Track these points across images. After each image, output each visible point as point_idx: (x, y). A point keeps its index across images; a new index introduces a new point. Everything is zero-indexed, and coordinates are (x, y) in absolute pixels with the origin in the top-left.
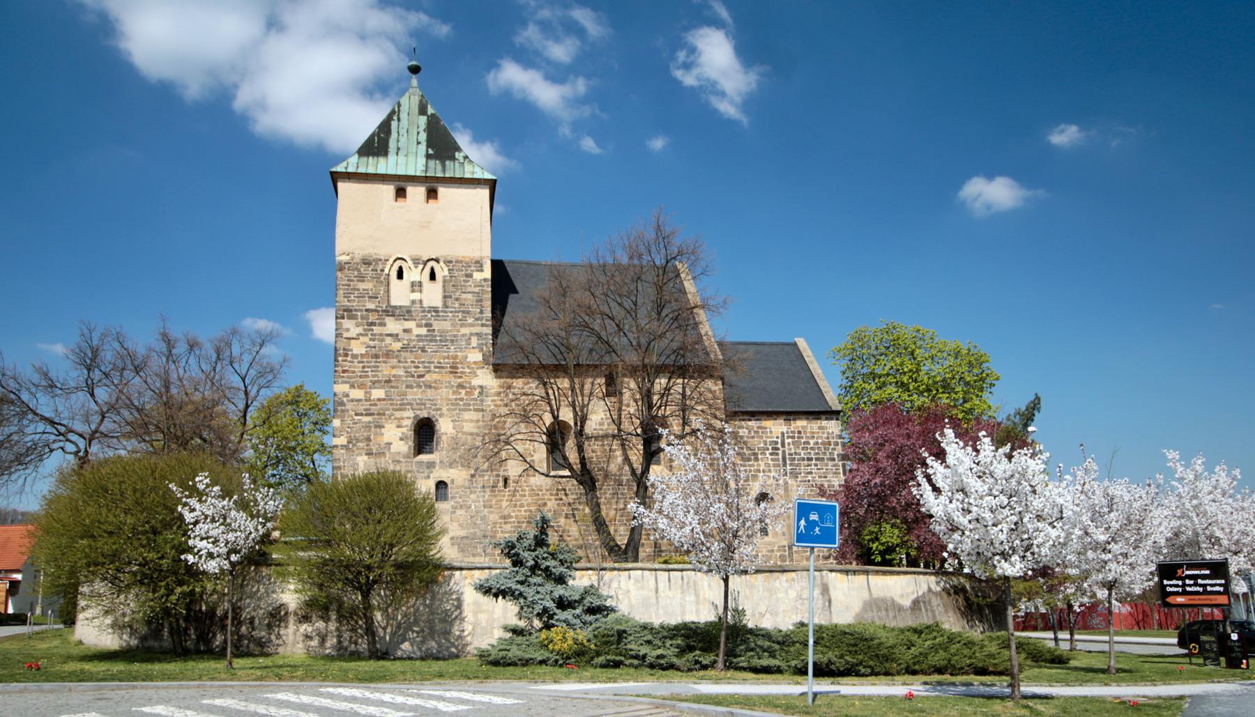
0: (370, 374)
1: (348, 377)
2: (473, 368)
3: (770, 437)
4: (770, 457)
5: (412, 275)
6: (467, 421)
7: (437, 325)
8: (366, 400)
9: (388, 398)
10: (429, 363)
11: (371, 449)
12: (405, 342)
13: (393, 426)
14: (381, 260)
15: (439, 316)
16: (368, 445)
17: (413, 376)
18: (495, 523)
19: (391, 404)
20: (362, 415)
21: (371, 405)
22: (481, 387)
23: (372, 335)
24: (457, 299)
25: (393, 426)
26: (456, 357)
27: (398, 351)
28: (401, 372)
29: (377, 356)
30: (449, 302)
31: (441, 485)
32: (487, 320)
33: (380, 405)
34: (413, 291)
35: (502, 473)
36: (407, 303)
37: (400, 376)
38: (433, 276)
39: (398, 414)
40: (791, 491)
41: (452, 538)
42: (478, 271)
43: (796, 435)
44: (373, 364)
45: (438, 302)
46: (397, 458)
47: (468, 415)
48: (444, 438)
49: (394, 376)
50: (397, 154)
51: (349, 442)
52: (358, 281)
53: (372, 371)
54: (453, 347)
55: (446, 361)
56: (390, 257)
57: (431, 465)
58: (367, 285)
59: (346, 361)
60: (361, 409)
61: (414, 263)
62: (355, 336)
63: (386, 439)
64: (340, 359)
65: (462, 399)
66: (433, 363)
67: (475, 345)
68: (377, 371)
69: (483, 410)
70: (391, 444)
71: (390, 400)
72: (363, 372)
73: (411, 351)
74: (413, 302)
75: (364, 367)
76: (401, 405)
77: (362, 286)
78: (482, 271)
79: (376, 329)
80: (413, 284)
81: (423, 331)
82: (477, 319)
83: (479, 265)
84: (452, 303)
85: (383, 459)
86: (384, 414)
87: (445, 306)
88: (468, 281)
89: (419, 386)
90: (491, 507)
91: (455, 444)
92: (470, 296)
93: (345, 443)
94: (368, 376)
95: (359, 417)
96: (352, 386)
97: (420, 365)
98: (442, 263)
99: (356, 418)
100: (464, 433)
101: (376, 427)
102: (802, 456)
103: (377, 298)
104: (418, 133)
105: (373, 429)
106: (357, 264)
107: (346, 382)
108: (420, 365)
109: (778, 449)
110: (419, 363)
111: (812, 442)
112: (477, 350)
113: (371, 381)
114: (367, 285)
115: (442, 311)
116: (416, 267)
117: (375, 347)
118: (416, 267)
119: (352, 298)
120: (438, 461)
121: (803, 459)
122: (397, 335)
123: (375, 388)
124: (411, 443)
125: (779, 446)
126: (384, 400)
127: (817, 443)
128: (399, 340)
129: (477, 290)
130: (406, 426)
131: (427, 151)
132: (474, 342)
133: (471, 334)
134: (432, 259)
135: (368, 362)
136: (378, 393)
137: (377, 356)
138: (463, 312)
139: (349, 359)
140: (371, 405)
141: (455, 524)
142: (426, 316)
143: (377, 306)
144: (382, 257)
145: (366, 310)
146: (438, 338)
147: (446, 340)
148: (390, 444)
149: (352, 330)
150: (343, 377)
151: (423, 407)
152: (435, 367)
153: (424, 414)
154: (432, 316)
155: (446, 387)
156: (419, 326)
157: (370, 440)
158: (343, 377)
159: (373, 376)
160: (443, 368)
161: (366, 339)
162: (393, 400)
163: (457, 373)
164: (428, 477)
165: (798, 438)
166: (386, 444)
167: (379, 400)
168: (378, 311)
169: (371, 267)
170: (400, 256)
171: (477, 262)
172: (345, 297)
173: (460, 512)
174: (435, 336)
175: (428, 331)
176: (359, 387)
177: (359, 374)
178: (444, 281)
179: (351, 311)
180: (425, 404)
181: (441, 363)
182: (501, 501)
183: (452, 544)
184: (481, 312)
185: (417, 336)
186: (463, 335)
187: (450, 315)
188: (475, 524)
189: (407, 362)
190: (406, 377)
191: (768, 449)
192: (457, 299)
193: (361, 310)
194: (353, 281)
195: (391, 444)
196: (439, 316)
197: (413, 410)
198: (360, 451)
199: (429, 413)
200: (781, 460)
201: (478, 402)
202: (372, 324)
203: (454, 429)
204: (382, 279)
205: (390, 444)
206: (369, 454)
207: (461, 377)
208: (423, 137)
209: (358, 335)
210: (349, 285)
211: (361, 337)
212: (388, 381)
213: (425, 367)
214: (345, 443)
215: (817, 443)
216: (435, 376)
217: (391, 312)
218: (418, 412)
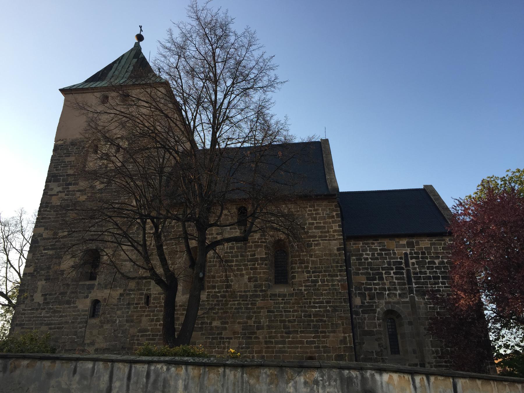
1: (44, 223)
3: (394, 258)
4: (394, 276)
18: (134, 336)
20: (48, 249)
23: (68, 191)
31: (96, 303)
35: (145, 292)
40: (419, 308)
43: (420, 256)
51: (34, 271)
52: (66, 156)
58: (72, 159)
59: (46, 211)
62: (55, 193)
77: (67, 159)
79: (71, 188)
90: (132, 321)
93: (32, 271)
95: (46, 251)
99: (44, 252)
102: (428, 275)
106: (67, 145)
109: (402, 269)
111: (437, 261)
119: (60, 168)
121: (429, 278)
125: (403, 266)
127: (443, 262)
141: (101, 337)
145: (68, 175)
149: (55, 189)
150: (42, 222)
158: (42, 222)
161: (63, 195)
164: (87, 297)
165: (422, 258)
177: (53, 219)
179: (57, 176)
182: (142, 316)
191: (392, 269)
194: (62, 157)
200: (406, 279)
201: (136, 235)
209: (58, 192)
211: (60, 194)
214: (32, 271)
215: (443, 262)
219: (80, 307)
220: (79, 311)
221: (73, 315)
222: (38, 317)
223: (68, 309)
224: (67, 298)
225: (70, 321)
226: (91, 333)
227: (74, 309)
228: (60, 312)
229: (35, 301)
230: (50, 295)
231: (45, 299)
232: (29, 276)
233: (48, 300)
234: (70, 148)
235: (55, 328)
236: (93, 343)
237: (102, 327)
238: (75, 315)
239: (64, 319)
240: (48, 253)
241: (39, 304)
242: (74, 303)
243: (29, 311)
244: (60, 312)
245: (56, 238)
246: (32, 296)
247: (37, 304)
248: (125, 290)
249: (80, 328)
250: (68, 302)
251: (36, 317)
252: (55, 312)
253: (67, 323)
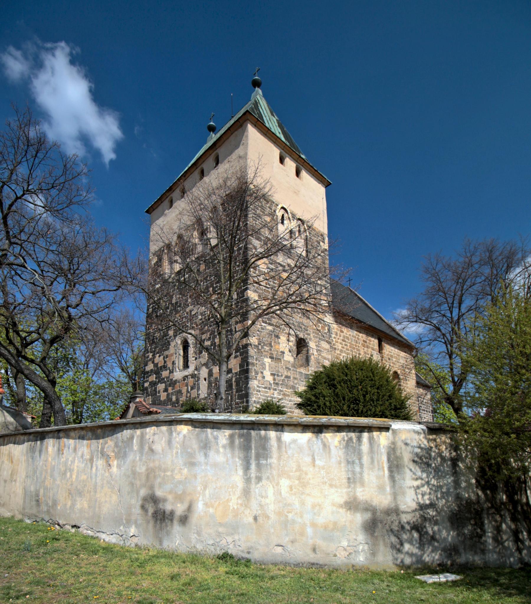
11: (272, 354)
16: (271, 350)
46: (288, 366)
198: (266, 353)
206: (272, 358)
229: (266, 379)
230: (278, 375)
231: (274, 379)
233: (277, 382)
243: (263, 389)
246: (262, 373)
247: (268, 383)
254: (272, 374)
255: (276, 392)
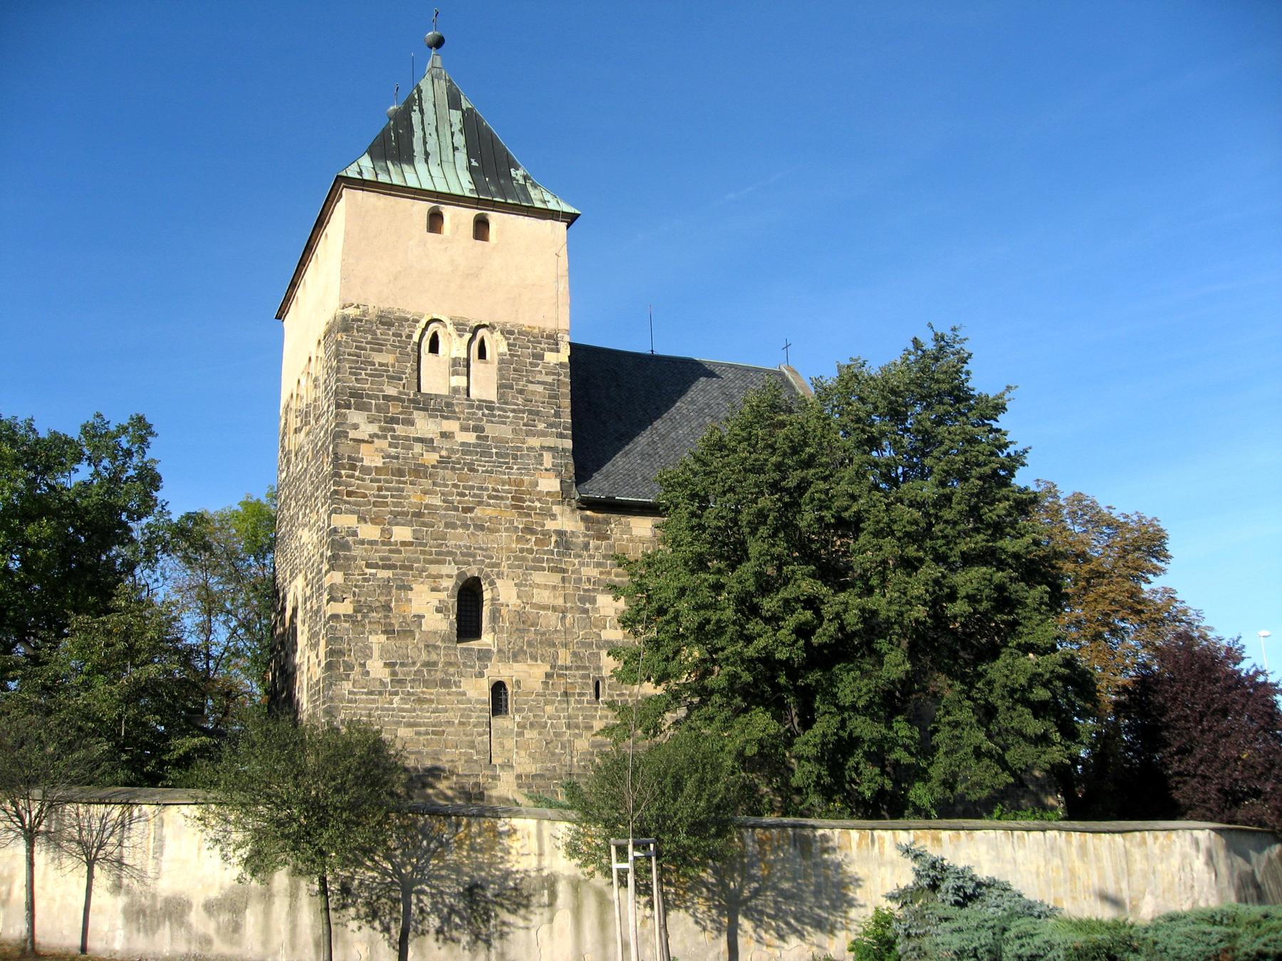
0: (389, 500)
1: (356, 504)
2: (547, 502)
5: (453, 346)
6: (538, 586)
7: (491, 430)
8: (384, 543)
9: (418, 541)
10: (481, 488)
11: (391, 624)
12: (444, 453)
13: (426, 588)
14: (407, 320)
15: (494, 416)
17: (456, 509)
19: (423, 552)
20: (376, 566)
21: (391, 551)
22: (560, 533)
23: (393, 437)
24: (521, 392)
25: (426, 588)
26: (522, 481)
27: (433, 467)
28: (437, 501)
29: (400, 473)
30: (510, 394)
31: (498, 689)
32: (565, 429)
33: (406, 553)
34: (455, 373)
36: (445, 392)
37: (437, 508)
38: (482, 354)
39: (434, 569)
41: (519, 777)
42: (552, 350)
44: (393, 485)
45: (491, 395)
47: (538, 577)
48: (504, 611)
49: (427, 506)
50: (426, 161)
51: (355, 611)
52: (372, 349)
53: (392, 496)
54: (515, 467)
55: (507, 487)
56: (422, 316)
57: (484, 655)
58: (387, 358)
59: (352, 476)
60: (376, 557)
61: (458, 330)
62: (366, 438)
63: (415, 608)
64: (343, 472)
65: (531, 551)
66: (487, 489)
67: (549, 466)
68: (400, 497)
69: (564, 571)
70: (424, 617)
71: (421, 544)
72: (379, 496)
73: (453, 469)
74: (456, 390)
75: (380, 489)
76: (438, 554)
77: (378, 358)
78: (558, 351)
79: (400, 429)
80: (455, 362)
81: (471, 438)
82: (550, 425)
83: (553, 341)
84: (513, 397)
85: (409, 641)
86: (411, 568)
87: (501, 397)
88: (537, 365)
89: (466, 526)
91: (523, 621)
92: (540, 388)
93: (350, 611)
94: (386, 504)
95: (373, 571)
96: (362, 519)
97: (467, 492)
98: (497, 335)
99: (368, 571)
100: (534, 606)
101: (399, 588)
103: (401, 379)
104: (453, 134)
105: (394, 591)
106: (371, 322)
107: (352, 512)
108: (467, 492)
110: (464, 487)
112: (552, 474)
113: (391, 512)
114: (387, 358)
115: (499, 409)
116: (461, 336)
117: (397, 458)
118: (461, 336)
119: (364, 376)
120: (495, 650)
122: (432, 440)
123: (397, 524)
124: (453, 617)
126: (411, 544)
128: (434, 449)
129: (549, 379)
130: (446, 589)
131: (470, 162)
132: (548, 460)
133: (542, 448)
134: (484, 326)
135: (386, 481)
136: (402, 533)
137: (400, 473)
138: (530, 412)
139: (357, 474)
140: (391, 551)
142: (474, 414)
143: (400, 393)
144: (409, 316)
145: (386, 397)
146: (494, 450)
147: (510, 454)
148: (421, 617)
149: (362, 427)
150: (349, 503)
151: (471, 559)
152: (490, 497)
153: (473, 571)
154: (483, 415)
155: (507, 530)
156: (464, 429)
157: (391, 609)
158: (349, 503)
159: (395, 504)
160: (502, 498)
161: (383, 444)
162: (425, 545)
163: (522, 508)
164: (481, 675)
166: (414, 616)
167: (404, 544)
168: (403, 401)
169: (393, 330)
170: (436, 316)
171: (550, 337)
172: (350, 373)
173: (529, 734)
174: (489, 447)
175: (478, 438)
176: (374, 522)
177: (373, 499)
178: (501, 362)
179: (361, 396)
180: (474, 556)
181: (494, 490)
183: (520, 786)
184: (557, 415)
185: (463, 444)
186: (530, 449)
187: (511, 415)
188: (553, 754)
189: (446, 486)
190: (447, 509)
192: (521, 392)
193: (377, 397)
195: (424, 617)
196: (494, 416)
197: (456, 563)
198: (375, 626)
199: (481, 570)
202: (394, 420)
203: (519, 597)
204: (409, 349)
205: (421, 617)
206: (389, 632)
207: (529, 515)
208: (460, 140)
209: (370, 436)
210: (359, 356)
211: (376, 440)
212: (419, 515)
213: (475, 496)
214: (350, 611)
216: (489, 511)
217: (424, 403)
218: (464, 568)
219: (472, 694)
220: (469, 701)
221: (460, 709)
222: (387, 710)
223: (448, 697)
224: (439, 675)
225: (457, 721)
226: (502, 745)
227: (460, 698)
228: (431, 701)
229: (372, 675)
230: (402, 665)
231: (394, 674)
232: (345, 621)
233: (400, 677)
234: (378, 331)
235: (427, 733)
236: (508, 765)
237: (521, 734)
238: (465, 709)
239: (443, 717)
240: (379, 576)
241: (382, 683)
242: (457, 684)
243: (364, 697)
244: (431, 701)
245: (390, 543)
246: (363, 665)
247: (378, 683)
248: (553, 667)
249: (480, 735)
250: (446, 683)
251: (383, 709)
252: (420, 701)
253: (450, 723)
254: (386, 665)
255: (396, 699)
